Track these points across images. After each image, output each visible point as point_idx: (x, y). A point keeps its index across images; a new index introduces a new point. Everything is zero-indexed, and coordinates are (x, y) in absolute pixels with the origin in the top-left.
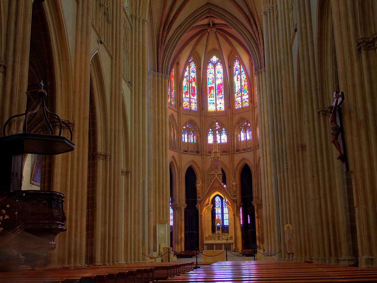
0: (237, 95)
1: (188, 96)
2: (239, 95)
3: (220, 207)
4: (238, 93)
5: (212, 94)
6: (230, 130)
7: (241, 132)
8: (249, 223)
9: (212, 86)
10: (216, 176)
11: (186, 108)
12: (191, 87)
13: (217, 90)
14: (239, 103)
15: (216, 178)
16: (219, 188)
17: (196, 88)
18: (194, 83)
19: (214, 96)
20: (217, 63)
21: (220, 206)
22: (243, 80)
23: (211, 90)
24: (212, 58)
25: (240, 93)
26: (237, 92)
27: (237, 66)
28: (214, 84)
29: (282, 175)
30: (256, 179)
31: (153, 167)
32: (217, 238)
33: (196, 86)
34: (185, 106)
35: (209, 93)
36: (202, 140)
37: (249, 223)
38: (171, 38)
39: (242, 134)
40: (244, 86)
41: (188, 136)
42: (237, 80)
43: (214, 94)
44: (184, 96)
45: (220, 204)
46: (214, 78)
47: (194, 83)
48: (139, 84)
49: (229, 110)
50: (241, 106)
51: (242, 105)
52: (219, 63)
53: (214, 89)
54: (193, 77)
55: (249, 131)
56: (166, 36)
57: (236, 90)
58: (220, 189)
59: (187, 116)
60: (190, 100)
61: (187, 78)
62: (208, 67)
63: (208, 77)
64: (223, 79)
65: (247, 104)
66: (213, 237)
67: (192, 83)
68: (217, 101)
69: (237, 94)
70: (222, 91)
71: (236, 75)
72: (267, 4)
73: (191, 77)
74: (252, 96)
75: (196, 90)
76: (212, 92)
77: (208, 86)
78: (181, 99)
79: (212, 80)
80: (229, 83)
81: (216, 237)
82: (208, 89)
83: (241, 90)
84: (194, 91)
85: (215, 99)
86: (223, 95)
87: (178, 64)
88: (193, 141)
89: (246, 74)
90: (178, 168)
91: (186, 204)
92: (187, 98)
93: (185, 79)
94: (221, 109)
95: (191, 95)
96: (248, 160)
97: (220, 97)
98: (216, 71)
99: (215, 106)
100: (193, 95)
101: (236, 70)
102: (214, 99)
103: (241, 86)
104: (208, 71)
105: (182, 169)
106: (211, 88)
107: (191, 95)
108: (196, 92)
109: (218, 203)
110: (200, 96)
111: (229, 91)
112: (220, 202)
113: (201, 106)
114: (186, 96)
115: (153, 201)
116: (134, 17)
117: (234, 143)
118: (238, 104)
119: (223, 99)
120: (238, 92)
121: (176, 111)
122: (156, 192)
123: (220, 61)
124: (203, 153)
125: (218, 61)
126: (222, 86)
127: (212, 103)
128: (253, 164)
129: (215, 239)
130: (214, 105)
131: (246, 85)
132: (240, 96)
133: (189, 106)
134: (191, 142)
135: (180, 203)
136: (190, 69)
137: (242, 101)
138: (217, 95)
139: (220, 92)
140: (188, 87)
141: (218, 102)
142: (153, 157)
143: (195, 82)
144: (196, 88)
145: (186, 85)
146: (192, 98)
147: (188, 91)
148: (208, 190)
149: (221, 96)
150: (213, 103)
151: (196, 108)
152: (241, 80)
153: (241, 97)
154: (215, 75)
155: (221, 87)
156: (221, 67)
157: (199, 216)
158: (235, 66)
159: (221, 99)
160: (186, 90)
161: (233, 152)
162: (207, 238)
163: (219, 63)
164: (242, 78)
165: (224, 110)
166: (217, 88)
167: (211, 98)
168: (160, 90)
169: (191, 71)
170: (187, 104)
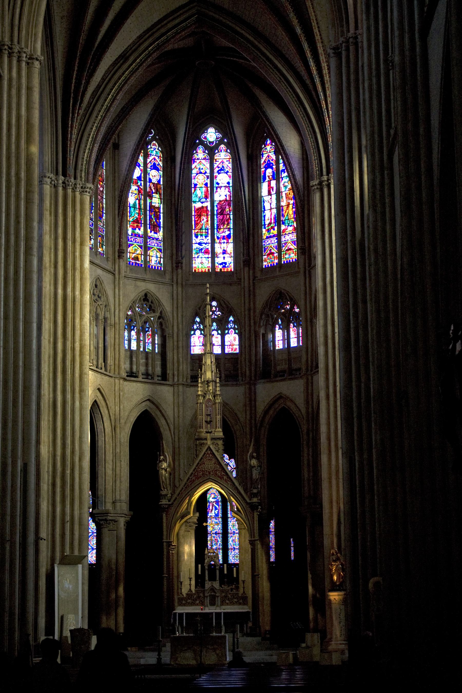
0: (268, 231)
3: (220, 515)
4: (270, 227)
5: (204, 228)
6: (247, 322)
7: (275, 327)
8: (292, 558)
9: (205, 205)
10: (209, 442)
14: (273, 254)
15: (209, 448)
16: (216, 475)
17: (162, 211)
18: (157, 196)
19: (210, 232)
21: (220, 512)
22: (284, 195)
23: (199, 216)
24: (204, 133)
25: (276, 228)
26: (267, 222)
27: (268, 156)
29: (365, 456)
30: (311, 450)
31: (49, 420)
32: (207, 601)
33: (162, 205)
34: (133, 257)
35: (196, 224)
36: (175, 347)
37: (292, 558)
38: (99, 87)
39: (279, 333)
40: (285, 208)
41: (138, 334)
42: (270, 194)
44: (130, 231)
45: (220, 507)
46: (209, 185)
47: (157, 196)
48: (18, 222)
49: (246, 269)
50: (276, 261)
51: (280, 258)
54: (154, 181)
55: (297, 327)
56: (88, 83)
57: (266, 218)
58: (218, 476)
60: (146, 243)
61: (139, 184)
62: (195, 156)
63: (194, 181)
64: (231, 188)
65: (293, 256)
67: (151, 198)
68: (217, 246)
69: (267, 228)
71: (267, 179)
72: (342, 26)
73: (150, 181)
74: (306, 235)
75: (162, 215)
76: (203, 222)
77: (194, 205)
78: (124, 240)
79: (204, 189)
80: (247, 202)
81: (207, 597)
83: (278, 220)
85: (209, 241)
86: (232, 230)
87: (116, 147)
88: (151, 348)
89: (292, 177)
90: (112, 418)
91: (130, 510)
92: (139, 236)
93: (134, 188)
94: (226, 266)
95: (149, 230)
96: (291, 401)
97: (223, 234)
98: (215, 166)
100: (155, 228)
101: (266, 168)
102: (209, 238)
103: (279, 208)
104: (193, 166)
105: (122, 421)
107: (149, 230)
108: (161, 221)
109: (213, 505)
110: (171, 231)
111: (248, 222)
112: (220, 504)
113: (174, 257)
115: (48, 507)
116: (5, 49)
117: (256, 355)
118: (268, 255)
119: (231, 240)
120: (270, 224)
121: (109, 272)
122: (54, 485)
123: (226, 140)
124: (176, 379)
125: (221, 142)
126: (229, 206)
127: (203, 251)
128: (303, 410)
129: (202, 604)
130: (207, 256)
131: (291, 206)
132: (274, 236)
133: (143, 256)
134: (147, 350)
135: (115, 507)
136: (149, 160)
137: (279, 247)
140: (142, 206)
141: (218, 249)
142: (49, 394)
143: (160, 194)
144: (162, 211)
145: (137, 201)
146: (150, 237)
147: (142, 217)
148: (187, 478)
149: (227, 233)
150: (206, 252)
151: (162, 262)
152: (279, 193)
153: (279, 236)
154: (212, 177)
156: (229, 156)
157: (165, 544)
158: (265, 156)
159: (225, 241)
160: (137, 216)
161: (253, 378)
162: (182, 599)
164: (283, 189)
168: (69, 221)
169: (149, 166)
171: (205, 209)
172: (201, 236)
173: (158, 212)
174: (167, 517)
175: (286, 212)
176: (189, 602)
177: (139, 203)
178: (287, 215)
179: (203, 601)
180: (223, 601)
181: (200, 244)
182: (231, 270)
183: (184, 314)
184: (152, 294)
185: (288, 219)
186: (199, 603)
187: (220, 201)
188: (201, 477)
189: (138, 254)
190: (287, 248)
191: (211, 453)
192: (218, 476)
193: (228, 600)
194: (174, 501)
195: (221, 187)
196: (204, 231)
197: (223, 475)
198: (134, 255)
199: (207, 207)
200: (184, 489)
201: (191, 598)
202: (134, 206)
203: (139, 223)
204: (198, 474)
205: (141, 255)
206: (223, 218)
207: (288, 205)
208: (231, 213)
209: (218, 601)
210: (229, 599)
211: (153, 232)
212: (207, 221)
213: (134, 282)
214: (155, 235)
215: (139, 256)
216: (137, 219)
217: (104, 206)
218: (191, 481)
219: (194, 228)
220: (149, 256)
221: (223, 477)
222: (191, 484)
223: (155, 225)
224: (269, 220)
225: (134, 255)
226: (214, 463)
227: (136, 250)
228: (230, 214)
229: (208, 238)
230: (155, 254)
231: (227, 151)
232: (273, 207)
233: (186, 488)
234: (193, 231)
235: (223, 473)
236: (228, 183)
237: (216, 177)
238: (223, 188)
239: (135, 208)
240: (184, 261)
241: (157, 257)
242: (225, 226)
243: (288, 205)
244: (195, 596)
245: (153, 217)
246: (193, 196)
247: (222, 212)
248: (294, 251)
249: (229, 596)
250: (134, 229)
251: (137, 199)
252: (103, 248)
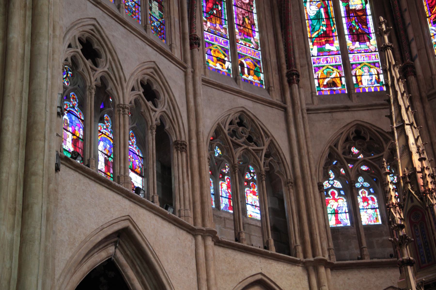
1: (336, 46)
11: (332, 91)
12: (343, 14)
17: (369, 12)
33: (368, 6)
34: (325, 83)
44: (314, 50)
59: (338, 115)
60: (345, 59)
75: (370, 18)
84: (365, 23)
95: (349, 43)
114: (328, 47)
133: (343, 79)
140: (332, 14)
144: (369, 12)
145: (322, 10)
146: (352, 52)
160: (324, 28)
170: (335, 74)
173: (363, 15)
177: (327, 13)
184: (368, 126)
189: (334, 78)
198: (327, 80)
202: (318, 17)
203: (330, 37)
205: (341, 77)
211: (357, 43)
213: (330, 115)
214: (363, 46)
215: (338, 81)
216: (325, 32)
217: (256, 22)
219: (428, 16)
220: (356, 76)
223: (360, 34)
225: (327, 80)
227: (329, 73)
230: (366, 71)
234: (428, 19)
239: (319, 19)
240: (417, 63)
241: (371, 75)
245: (354, 24)
250: (321, 45)
251: (322, 7)
252: (258, 77)
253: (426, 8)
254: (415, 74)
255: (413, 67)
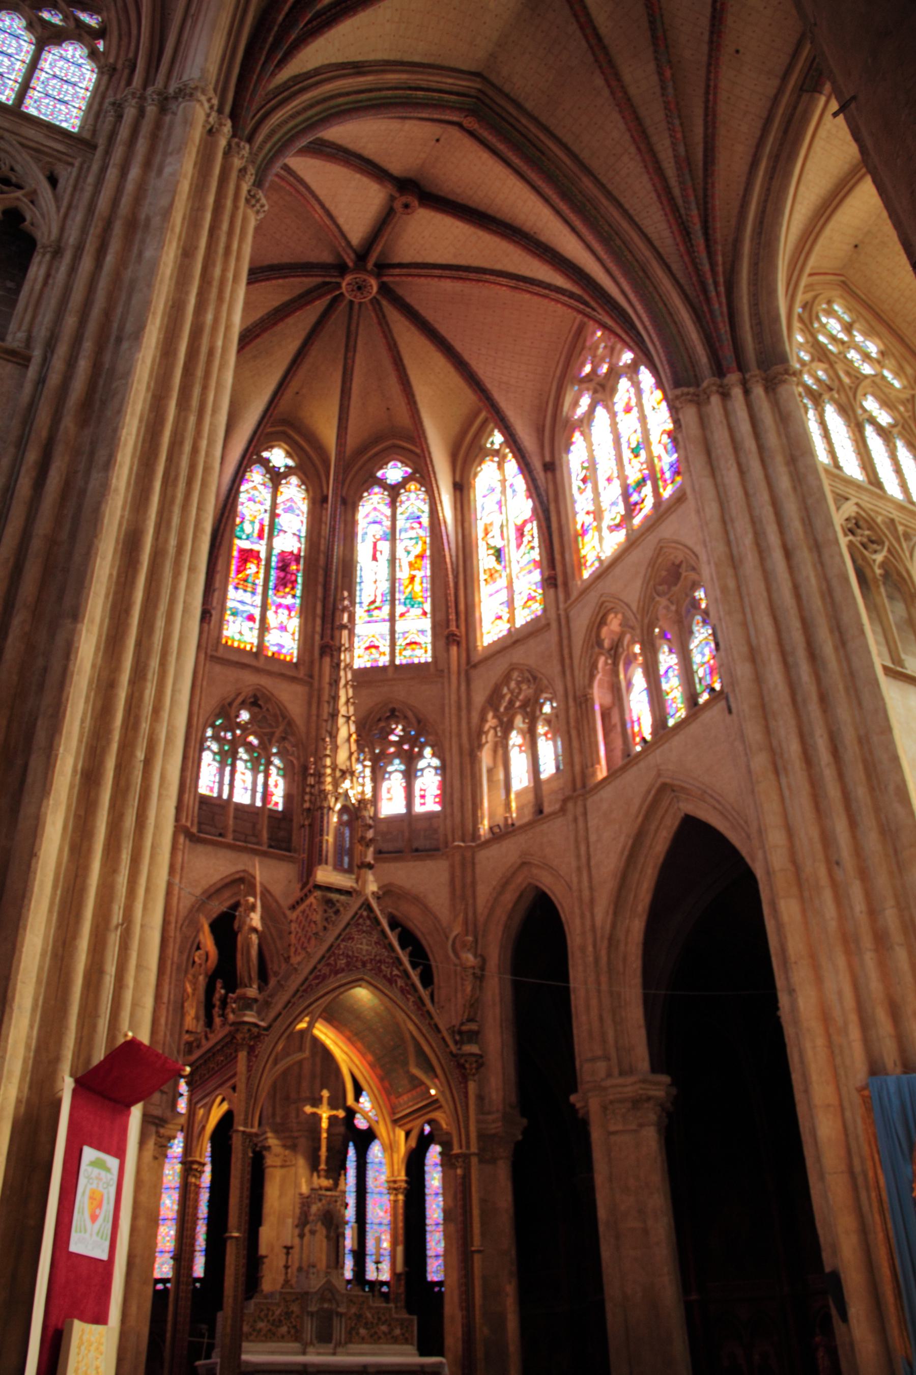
2: (376, 612)
9: (255, 547)
13: (273, 573)
16: (380, 971)
19: (260, 590)
20: (285, 476)
26: (366, 600)
28: (264, 542)
32: (309, 1328)
35: (238, 572)
42: (375, 558)
43: (257, 582)
52: (294, 480)
53: (263, 563)
58: (385, 976)
62: (248, 475)
64: (303, 540)
66: (288, 1314)
68: (270, 614)
69: (366, 608)
70: (296, 581)
76: (248, 572)
79: (257, 526)
82: (235, 553)
98: (279, 500)
99: (256, 633)
102: (258, 599)
104: (243, 488)
106: (247, 556)
120: (373, 602)
126: (298, 563)
127: (245, 615)
129: (296, 1335)
130: (251, 624)
131: (417, 580)
138: (271, 592)
139: (285, 581)
149: (289, 601)
150: (251, 618)
152: (393, 561)
153: (392, 619)
154: (274, 515)
155: (294, 567)
159: (286, 612)
163: (294, 480)
164: (400, 553)
165: (295, 660)
166: (273, 564)
167: (241, 591)
171: (255, 554)
172: (245, 591)
174: (249, 1060)
175: (407, 587)
176: (260, 1330)
178: (410, 593)
179: (298, 1327)
180: (352, 1329)
181: (241, 602)
182: (291, 660)
183: (203, 704)
185: (412, 598)
186: (289, 1332)
187: (283, 552)
188: (343, 970)
190: (408, 641)
191: (369, 917)
192: (385, 976)
193: (366, 1325)
194: (275, 1019)
195: (285, 532)
196: (250, 585)
197: (397, 975)
199: (258, 552)
200: (299, 994)
201: (267, 1315)
204: (336, 964)
206: (286, 576)
207: (412, 578)
208: (300, 574)
209: (339, 1329)
210: (366, 1324)
212: (257, 572)
218: (316, 977)
221: (396, 982)
222: (317, 985)
224: (372, 599)
226: (376, 943)
228: (297, 576)
229: (255, 598)
231: (300, 486)
232: (378, 577)
233: (305, 991)
235: (396, 972)
236: (299, 531)
237: (278, 515)
238: (289, 535)
242: (287, 590)
243: (412, 578)
244: (278, 1312)
246: (238, 529)
247: (284, 566)
248: (424, 646)
249: (369, 1315)
253: (233, 567)
254: (209, 623)
255: (211, 616)
